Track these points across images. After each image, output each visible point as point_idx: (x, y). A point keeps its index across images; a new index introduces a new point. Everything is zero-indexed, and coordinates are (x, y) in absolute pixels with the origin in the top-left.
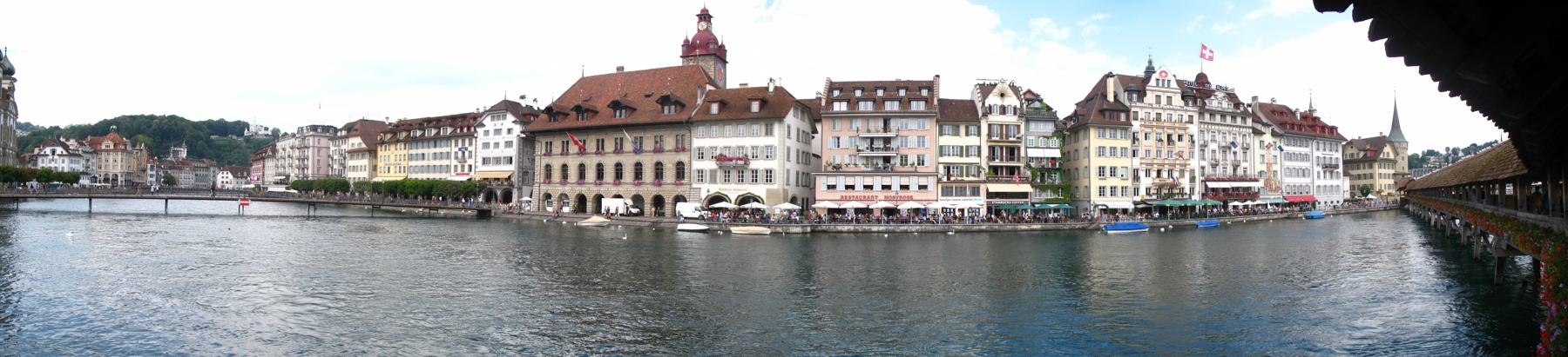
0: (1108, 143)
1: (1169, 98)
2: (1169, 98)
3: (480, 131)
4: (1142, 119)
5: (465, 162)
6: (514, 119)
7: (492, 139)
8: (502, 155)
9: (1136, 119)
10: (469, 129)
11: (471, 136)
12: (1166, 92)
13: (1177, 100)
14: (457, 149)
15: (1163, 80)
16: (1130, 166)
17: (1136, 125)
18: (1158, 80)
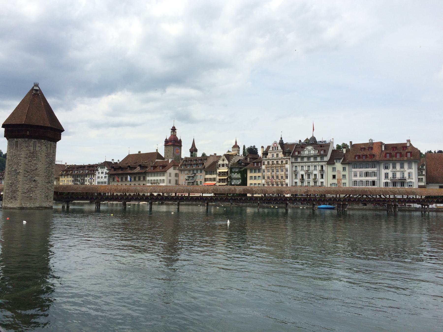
0: (253, 175)
1: (277, 155)
2: (277, 155)
3: (97, 172)
4: (266, 165)
5: (92, 183)
6: (107, 169)
7: (101, 175)
8: (103, 181)
9: (264, 164)
10: (93, 171)
11: (94, 175)
12: (275, 152)
13: (281, 155)
14: (89, 179)
15: (275, 147)
16: (261, 183)
17: (263, 167)
18: (273, 148)
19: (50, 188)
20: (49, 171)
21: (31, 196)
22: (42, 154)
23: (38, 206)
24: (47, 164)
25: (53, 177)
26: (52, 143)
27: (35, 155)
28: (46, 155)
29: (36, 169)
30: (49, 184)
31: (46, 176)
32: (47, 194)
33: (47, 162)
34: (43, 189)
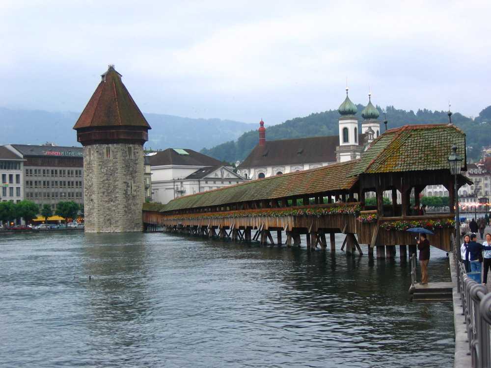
19: (114, 208)
20: (109, 184)
21: (91, 221)
22: (95, 163)
23: (96, 231)
24: (104, 176)
25: (118, 192)
26: (110, 145)
27: (91, 166)
28: (99, 165)
29: (92, 184)
30: (112, 203)
31: (104, 193)
32: (108, 217)
33: (103, 173)
34: (99, 211)
